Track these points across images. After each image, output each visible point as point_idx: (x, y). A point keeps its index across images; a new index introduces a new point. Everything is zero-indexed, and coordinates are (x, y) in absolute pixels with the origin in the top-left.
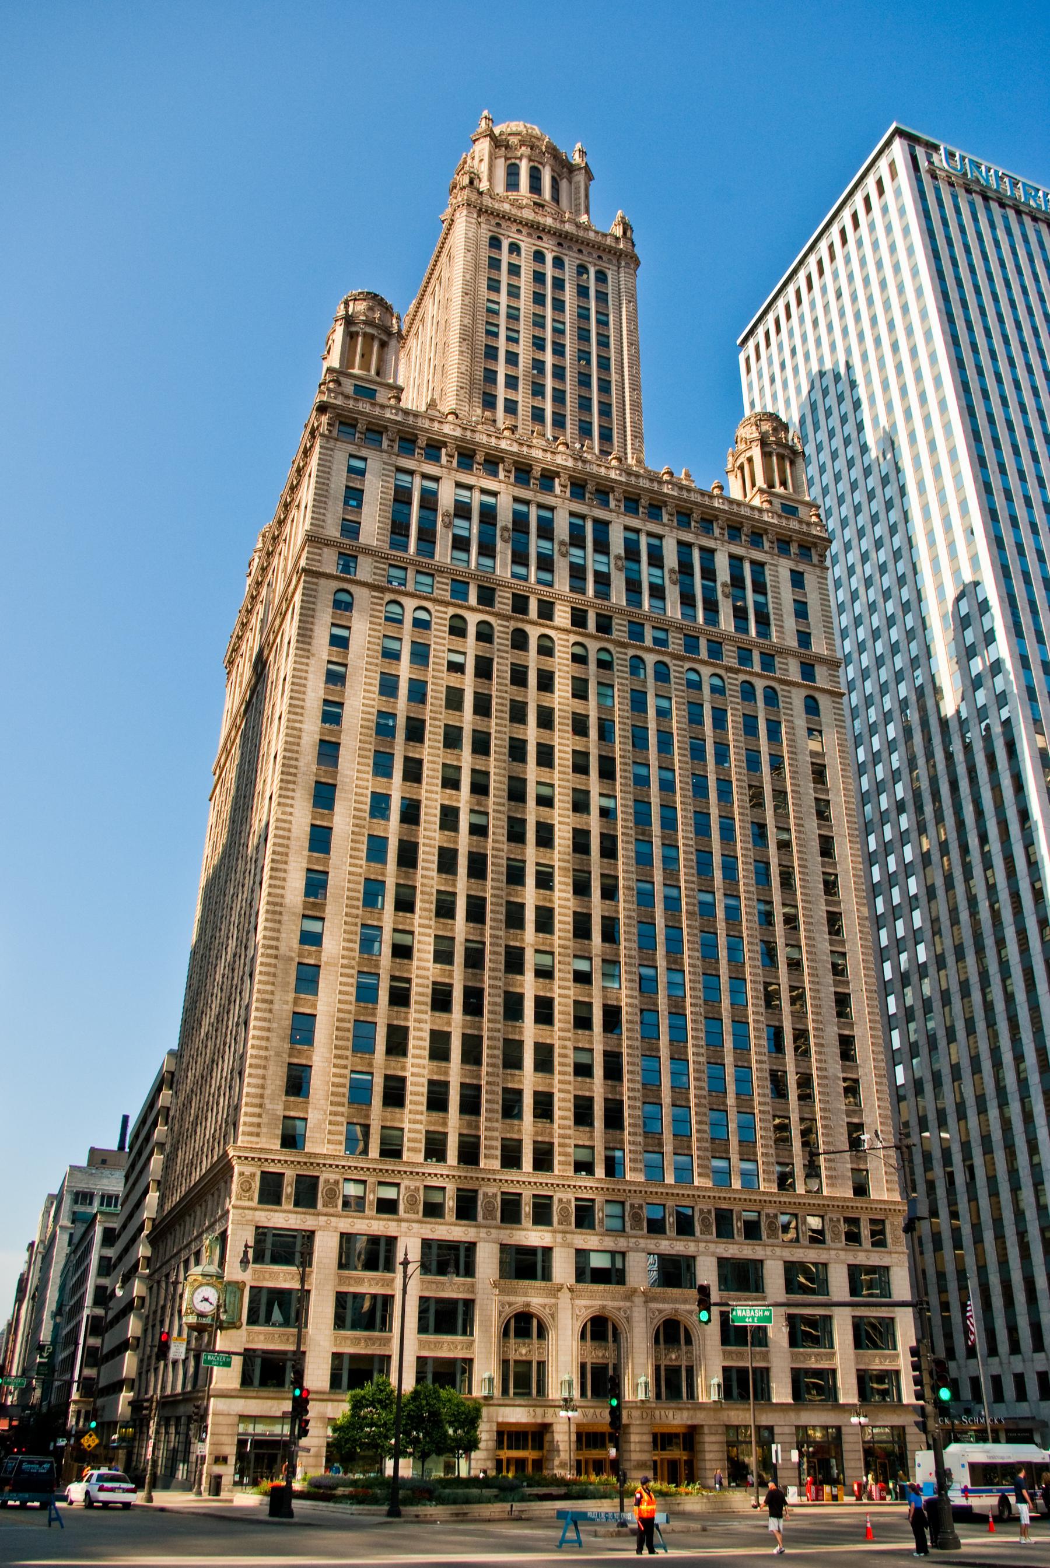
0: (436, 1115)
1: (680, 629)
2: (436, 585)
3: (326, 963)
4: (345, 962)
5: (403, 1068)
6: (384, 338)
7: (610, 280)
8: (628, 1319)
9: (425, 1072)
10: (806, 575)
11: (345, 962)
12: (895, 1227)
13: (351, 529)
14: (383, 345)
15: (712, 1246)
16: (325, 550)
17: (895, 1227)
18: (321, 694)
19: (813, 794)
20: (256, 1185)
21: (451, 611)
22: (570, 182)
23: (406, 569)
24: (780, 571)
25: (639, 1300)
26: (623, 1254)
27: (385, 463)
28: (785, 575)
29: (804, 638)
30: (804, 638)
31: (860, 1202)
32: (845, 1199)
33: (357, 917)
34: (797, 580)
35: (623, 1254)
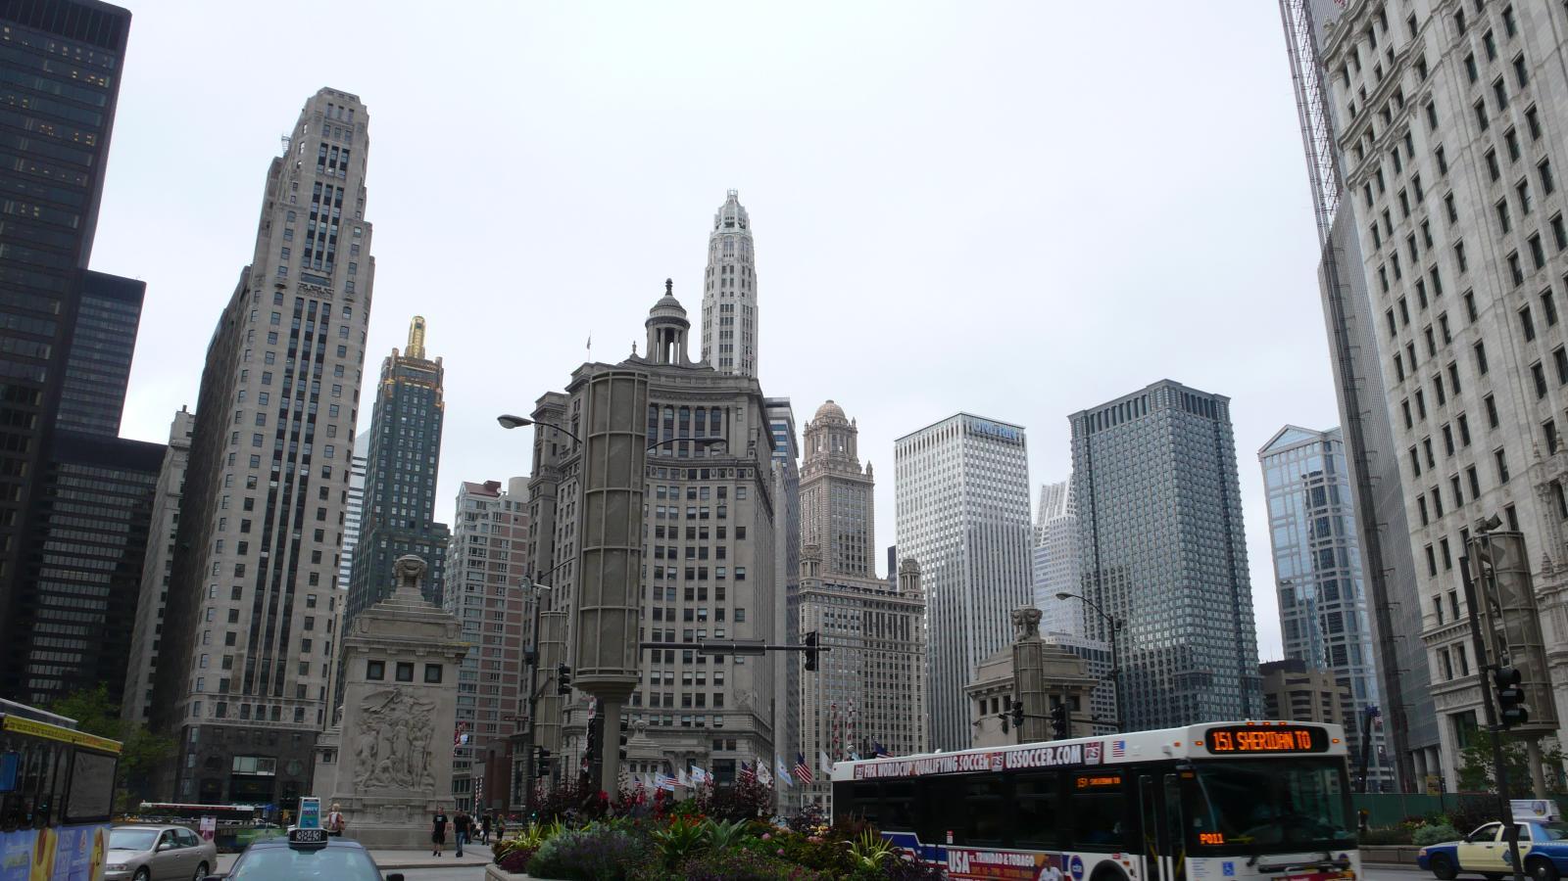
24: (913, 617)
28: (913, 619)
29: (917, 639)
30: (917, 639)
34: (917, 619)
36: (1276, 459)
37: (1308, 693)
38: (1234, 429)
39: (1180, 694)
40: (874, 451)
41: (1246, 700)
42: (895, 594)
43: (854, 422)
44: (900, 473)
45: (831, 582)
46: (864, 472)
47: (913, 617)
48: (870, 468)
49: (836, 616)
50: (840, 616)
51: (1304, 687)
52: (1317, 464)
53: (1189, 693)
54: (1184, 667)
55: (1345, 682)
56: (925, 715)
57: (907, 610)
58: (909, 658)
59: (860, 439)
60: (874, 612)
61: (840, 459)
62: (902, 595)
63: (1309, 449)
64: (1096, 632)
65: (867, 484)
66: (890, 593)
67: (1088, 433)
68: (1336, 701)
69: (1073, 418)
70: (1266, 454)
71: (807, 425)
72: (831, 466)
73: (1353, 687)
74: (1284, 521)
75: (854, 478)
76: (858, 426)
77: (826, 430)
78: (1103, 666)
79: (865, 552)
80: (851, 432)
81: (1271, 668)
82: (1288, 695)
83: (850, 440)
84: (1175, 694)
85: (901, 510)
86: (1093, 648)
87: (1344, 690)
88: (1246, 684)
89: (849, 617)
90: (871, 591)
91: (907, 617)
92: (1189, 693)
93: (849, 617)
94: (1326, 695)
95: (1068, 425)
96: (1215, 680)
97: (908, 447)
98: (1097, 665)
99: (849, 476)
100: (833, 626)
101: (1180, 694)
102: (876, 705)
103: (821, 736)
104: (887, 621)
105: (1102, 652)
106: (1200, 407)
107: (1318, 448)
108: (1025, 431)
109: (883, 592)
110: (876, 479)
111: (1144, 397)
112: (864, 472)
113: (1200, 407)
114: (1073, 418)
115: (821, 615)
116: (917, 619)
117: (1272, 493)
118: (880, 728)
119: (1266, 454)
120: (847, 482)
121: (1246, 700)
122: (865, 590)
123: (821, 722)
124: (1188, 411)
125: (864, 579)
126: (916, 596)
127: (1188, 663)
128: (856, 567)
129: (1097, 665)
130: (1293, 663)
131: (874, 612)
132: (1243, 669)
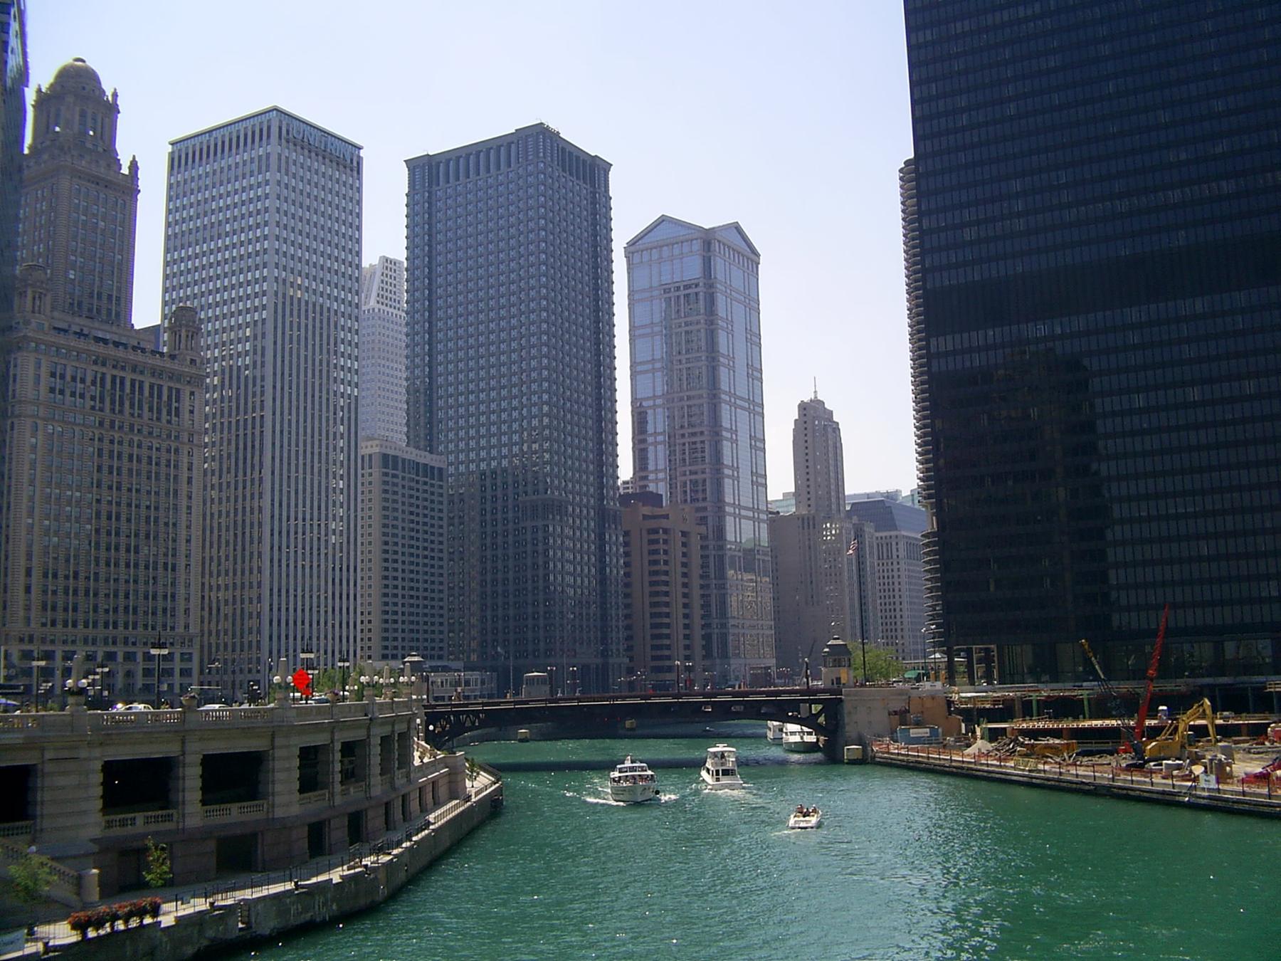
12: (197, 641)
17: (197, 641)
34: (192, 393)
36: (646, 255)
37: (666, 531)
38: (613, 203)
39: (529, 524)
40: (144, 143)
41: (601, 536)
42: (162, 354)
43: (115, 95)
44: (175, 193)
45: (65, 326)
46: (125, 171)
47: (188, 389)
48: (134, 166)
49: (68, 378)
50: (74, 379)
51: (664, 523)
52: (692, 270)
53: (540, 523)
54: (536, 492)
55: (703, 521)
56: (196, 533)
57: (179, 381)
58: (177, 450)
59: (122, 121)
60: (129, 377)
61: (89, 146)
62: (172, 357)
63: (686, 249)
64: (422, 444)
65: (128, 188)
66: (154, 352)
67: (430, 185)
68: (695, 542)
69: (412, 165)
70: (633, 248)
72: (74, 153)
73: (710, 529)
74: (648, 330)
77: (70, 99)
78: (432, 486)
79: (118, 304)
80: (111, 109)
81: (625, 499)
82: (644, 533)
84: (522, 525)
85: (174, 242)
86: (422, 461)
87: (703, 529)
88: (604, 517)
90: (125, 346)
91: (178, 391)
92: (540, 523)
94: (684, 534)
95: (405, 172)
96: (570, 509)
97: (189, 156)
98: (425, 483)
99: (102, 171)
100: (62, 392)
101: (529, 524)
102: (123, 518)
103: (35, 559)
104: (146, 393)
105: (433, 468)
106: (578, 168)
107: (697, 246)
108: (362, 153)
109: (143, 350)
110: (141, 184)
111: (509, 145)
112: (125, 171)
113: (578, 168)
114: (412, 165)
115: (44, 371)
116: (192, 393)
117: (636, 297)
118: (128, 551)
119: (632, 249)
120: (97, 181)
121: (601, 536)
122: (117, 344)
124: (564, 170)
125: (114, 328)
126: (193, 361)
127: (530, 489)
128: (104, 312)
129: (425, 483)
130: (641, 495)
131: (129, 377)
132: (602, 498)
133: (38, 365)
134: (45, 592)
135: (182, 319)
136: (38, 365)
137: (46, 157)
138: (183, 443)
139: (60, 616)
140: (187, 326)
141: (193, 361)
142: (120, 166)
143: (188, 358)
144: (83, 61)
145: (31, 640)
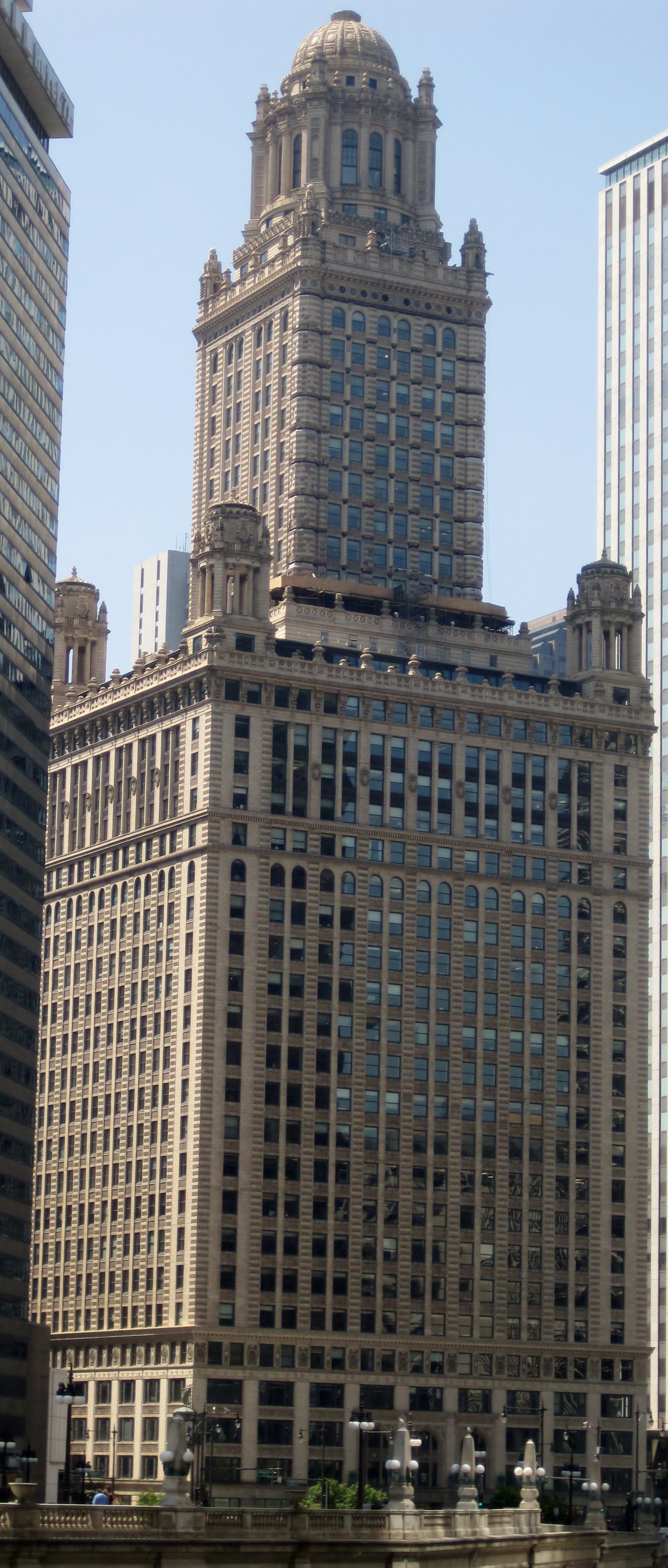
0: (317, 1297)
1: (510, 853)
2: (310, 842)
3: (243, 1189)
4: (254, 1186)
5: (296, 1264)
6: (257, 564)
7: (459, 342)
8: (444, 1434)
9: (310, 1265)
10: (629, 770)
11: (254, 1186)
13: (240, 800)
14: (256, 571)
15: (504, 1383)
16: (222, 822)
18: (226, 964)
19: (611, 1001)
20: (206, 1351)
21: (321, 867)
22: (414, 141)
23: (285, 830)
25: (451, 1421)
26: (442, 1389)
27: (265, 720)
28: (609, 773)
31: (616, 1348)
32: (604, 1347)
33: (261, 1150)
35: (442, 1389)
43: (427, 85)
46: (455, 260)
57: (585, 742)
62: (569, 688)
71: (264, 100)
75: (416, 276)
76: (443, 102)
83: (409, 149)
89: (364, 759)
93: (364, 759)
99: (394, 272)
103: (244, 1174)
112: (455, 260)
118: (467, 1152)
123: (245, 1124)
126: (620, 696)
133: (242, 729)
134: (268, 1245)
135: (606, 599)
136: (242, 729)
137: (273, 251)
138: (598, 892)
139: (304, 1301)
140: (603, 612)
141: (620, 696)
142: (444, 251)
143: (609, 689)
144: (355, 17)
145: (237, 1357)
